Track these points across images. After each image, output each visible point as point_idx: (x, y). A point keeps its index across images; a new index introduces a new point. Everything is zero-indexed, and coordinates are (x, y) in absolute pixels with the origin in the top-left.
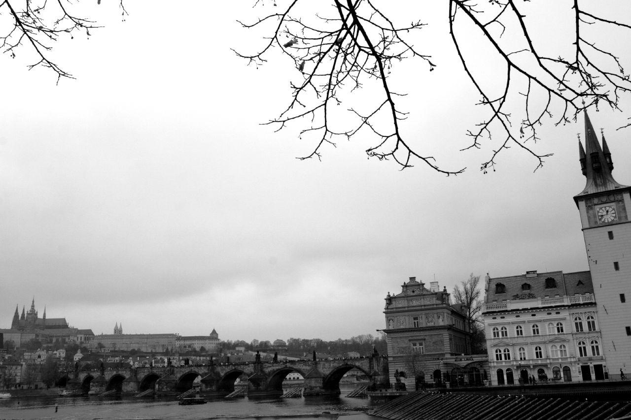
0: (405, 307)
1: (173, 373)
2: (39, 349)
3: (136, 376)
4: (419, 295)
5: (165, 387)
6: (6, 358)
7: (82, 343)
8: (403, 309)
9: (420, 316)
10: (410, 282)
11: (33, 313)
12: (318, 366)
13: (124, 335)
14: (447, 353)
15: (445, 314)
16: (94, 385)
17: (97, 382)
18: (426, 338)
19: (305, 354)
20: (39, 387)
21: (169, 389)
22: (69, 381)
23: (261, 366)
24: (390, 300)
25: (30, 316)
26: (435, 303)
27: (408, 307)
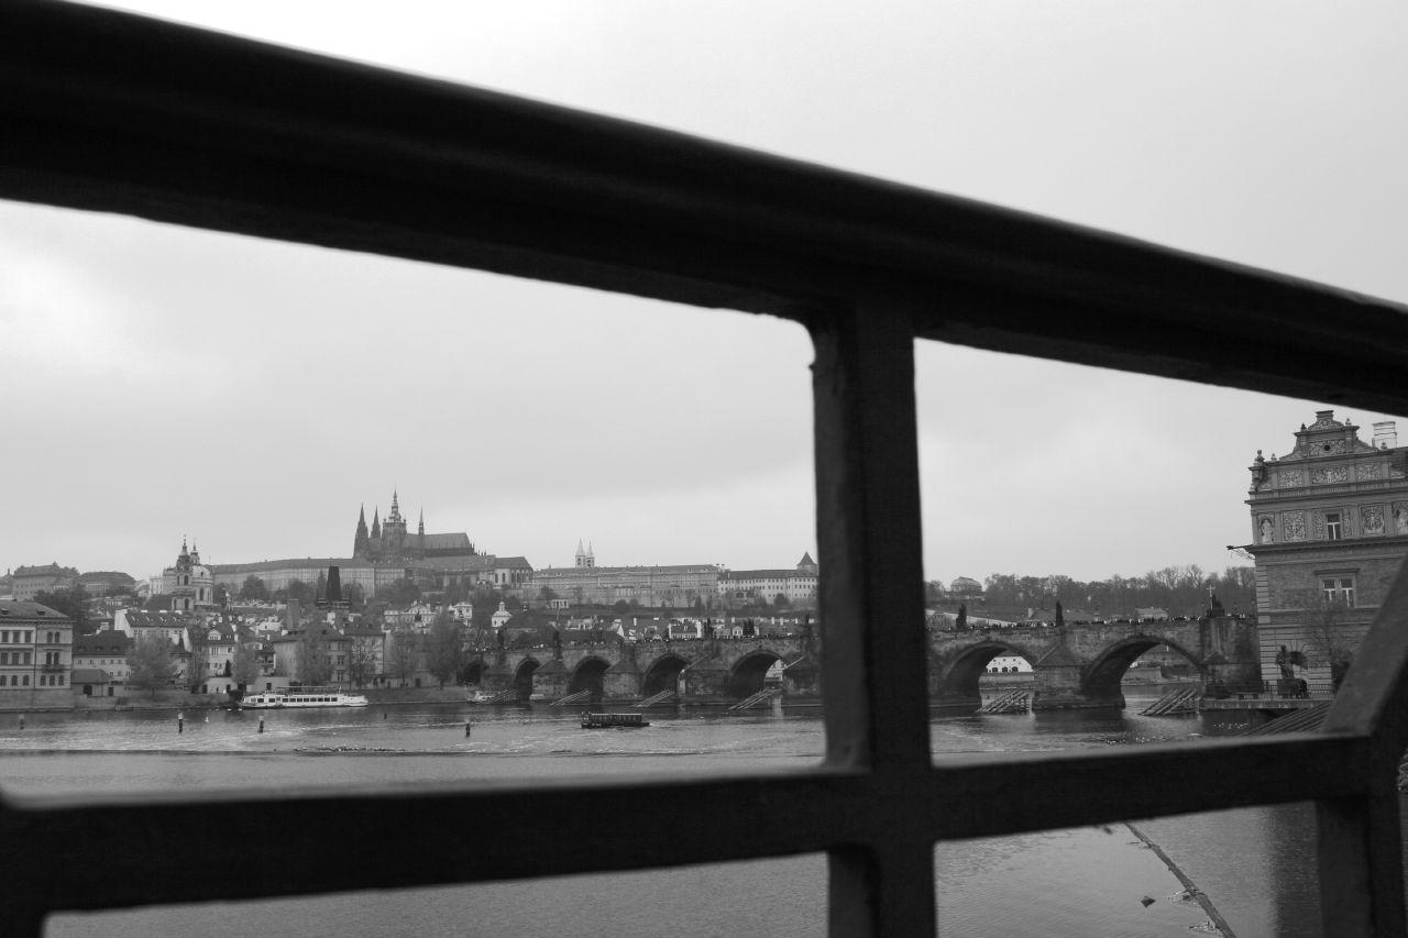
0: (1303, 489)
1: (717, 654)
2: (415, 603)
4: (1344, 458)
5: (701, 685)
6: (351, 620)
7: (505, 587)
8: (1299, 494)
9: (1346, 511)
10: (1317, 424)
11: (397, 524)
12: (1069, 638)
13: (598, 569)
16: (542, 679)
17: (548, 674)
18: (1363, 567)
19: (1030, 612)
20: (423, 685)
21: (710, 692)
22: (487, 672)
24: (1263, 470)
25: (391, 530)
26: (1386, 476)
27: (1312, 488)
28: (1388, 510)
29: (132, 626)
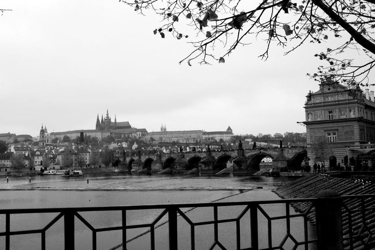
0: (321, 103)
2: (112, 142)
3: (160, 159)
5: (179, 166)
6: (80, 148)
7: (140, 138)
8: (320, 105)
9: (334, 110)
11: (108, 119)
12: (284, 152)
13: (167, 132)
14: (356, 142)
15: (357, 109)
17: (136, 163)
18: (339, 129)
19: (289, 144)
20: (102, 167)
21: (181, 168)
22: (120, 163)
23: (243, 152)
24: (310, 96)
25: (106, 121)
26: (347, 98)
27: (324, 103)
28: (348, 109)
29: (15, 151)
